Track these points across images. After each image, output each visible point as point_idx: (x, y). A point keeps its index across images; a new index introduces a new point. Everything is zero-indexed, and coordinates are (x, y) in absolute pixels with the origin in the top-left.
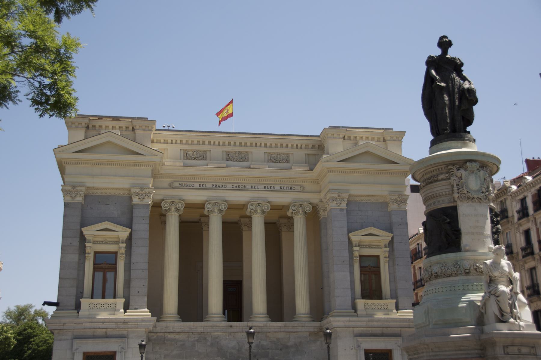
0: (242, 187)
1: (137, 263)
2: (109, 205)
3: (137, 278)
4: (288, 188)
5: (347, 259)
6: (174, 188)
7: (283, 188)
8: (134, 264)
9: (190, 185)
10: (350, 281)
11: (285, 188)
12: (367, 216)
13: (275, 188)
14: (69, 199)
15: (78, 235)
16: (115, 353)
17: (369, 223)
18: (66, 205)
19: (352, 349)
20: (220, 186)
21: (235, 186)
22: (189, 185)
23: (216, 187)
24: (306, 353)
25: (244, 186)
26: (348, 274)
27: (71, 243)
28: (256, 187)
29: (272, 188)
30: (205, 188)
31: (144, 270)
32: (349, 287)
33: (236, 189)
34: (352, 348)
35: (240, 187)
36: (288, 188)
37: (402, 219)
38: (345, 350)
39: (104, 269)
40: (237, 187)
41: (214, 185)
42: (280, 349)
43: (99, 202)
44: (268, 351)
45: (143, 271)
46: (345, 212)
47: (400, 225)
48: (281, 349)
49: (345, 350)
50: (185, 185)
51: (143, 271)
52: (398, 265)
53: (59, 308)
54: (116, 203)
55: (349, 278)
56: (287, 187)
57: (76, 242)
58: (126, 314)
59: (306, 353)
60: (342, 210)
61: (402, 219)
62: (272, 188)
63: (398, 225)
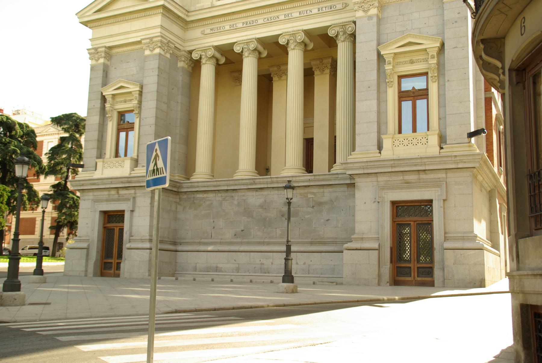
0: (274, 18)
1: (146, 118)
2: (129, 63)
3: (145, 135)
4: (327, 8)
5: (375, 82)
6: (206, 34)
7: (321, 10)
8: (143, 120)
9: (221, 28)
10: (376, 112)
11: (324, 9)
12: (412, 20)
13: (311, 12)
14: (94, 62)
15: (99, 97)
16: (124, 211)
17: (414, 29)
18: (93, 68)
19: (375, 202)
20: (251, 23)
21: (267, 19)
22: (220, 28)
23: (246, 24)
24: (343, 210)
25: (276, 17)
26: (375, 102)
27: (94, 106)
28: (290, 15)
29: (308, 12)
30: (236, 28)
31: (151, 126)
32: (376, 119)
33: (268, 22)
34: (375, 200)
35: (272, 18)
36: (327, 8)
37: (459, 13)
38: (365, 203)
39: (126, 129)
40: (269, 19)
41: (245, 23)
42: (312, 206)
43: (122, 61)
44: (297, 209)
45: (151, 127)
46: (375, 19)
47: (456, 22)
48: (313, 207)
49: (365, 203)
50: (216, 29)
51: (151, 127)
52: (448, 81)
53: (84, 169)
54: (135, 60)
55: (375, 108)
56: (326, 7)
57: (98, 104)
58: (133, 172)
59: (343, 210)
60: (370, 18)
61: (459, 13)
62: (308, 12)
63: (453, 24)
